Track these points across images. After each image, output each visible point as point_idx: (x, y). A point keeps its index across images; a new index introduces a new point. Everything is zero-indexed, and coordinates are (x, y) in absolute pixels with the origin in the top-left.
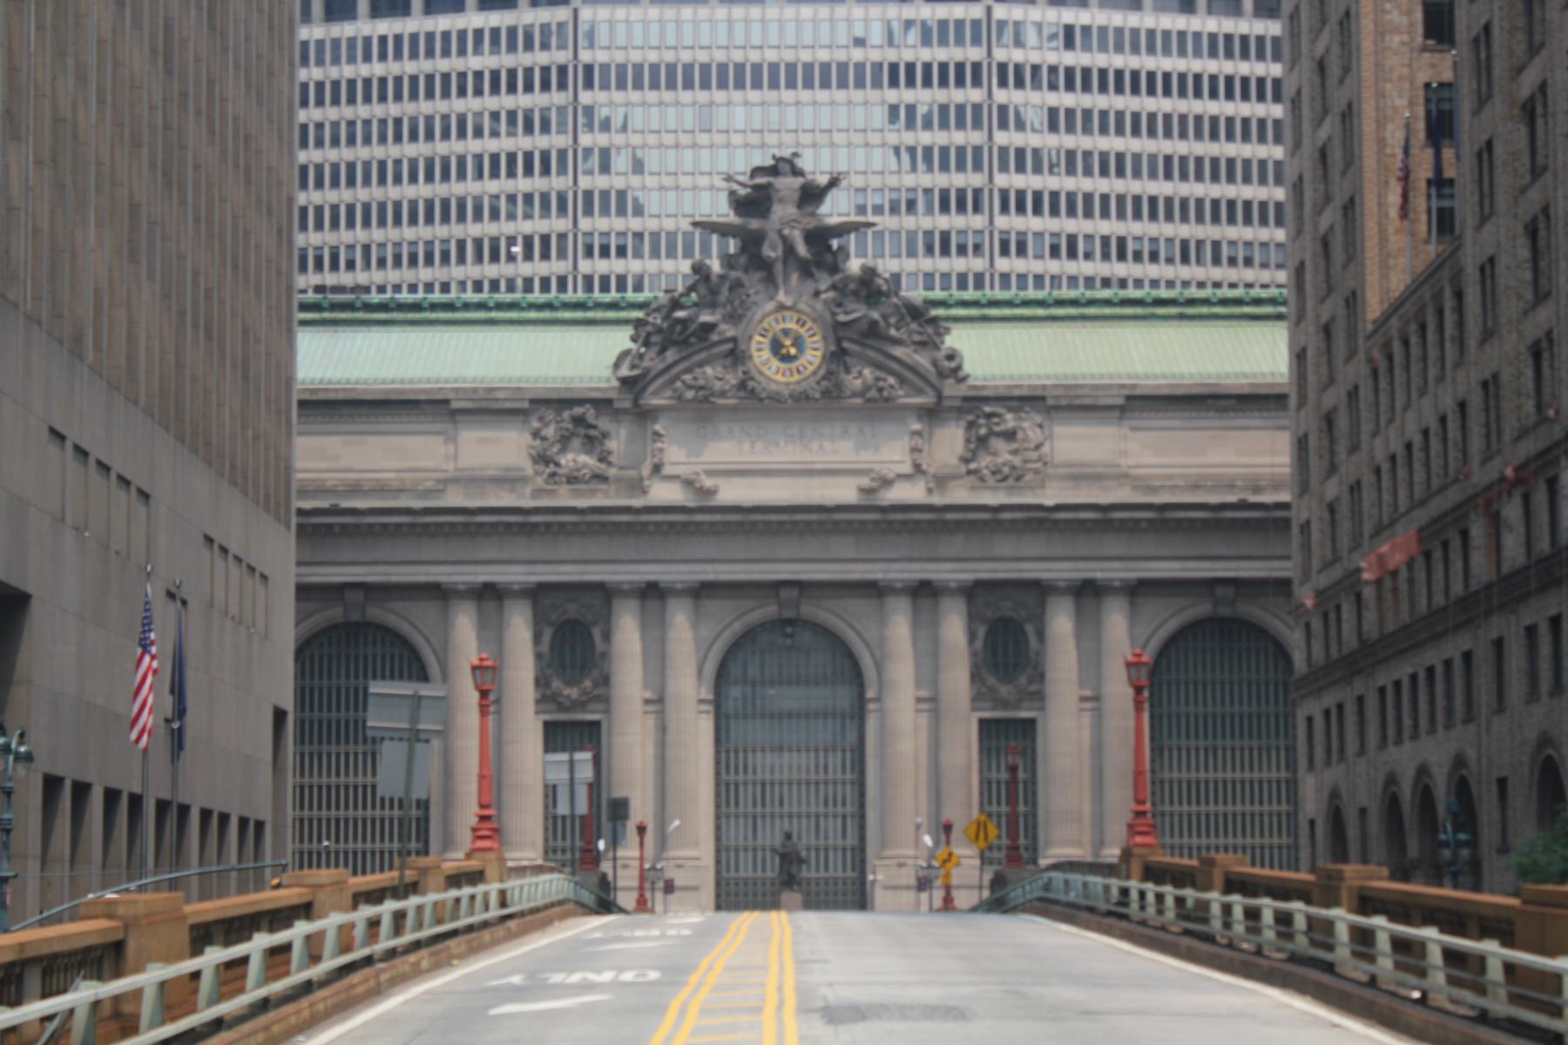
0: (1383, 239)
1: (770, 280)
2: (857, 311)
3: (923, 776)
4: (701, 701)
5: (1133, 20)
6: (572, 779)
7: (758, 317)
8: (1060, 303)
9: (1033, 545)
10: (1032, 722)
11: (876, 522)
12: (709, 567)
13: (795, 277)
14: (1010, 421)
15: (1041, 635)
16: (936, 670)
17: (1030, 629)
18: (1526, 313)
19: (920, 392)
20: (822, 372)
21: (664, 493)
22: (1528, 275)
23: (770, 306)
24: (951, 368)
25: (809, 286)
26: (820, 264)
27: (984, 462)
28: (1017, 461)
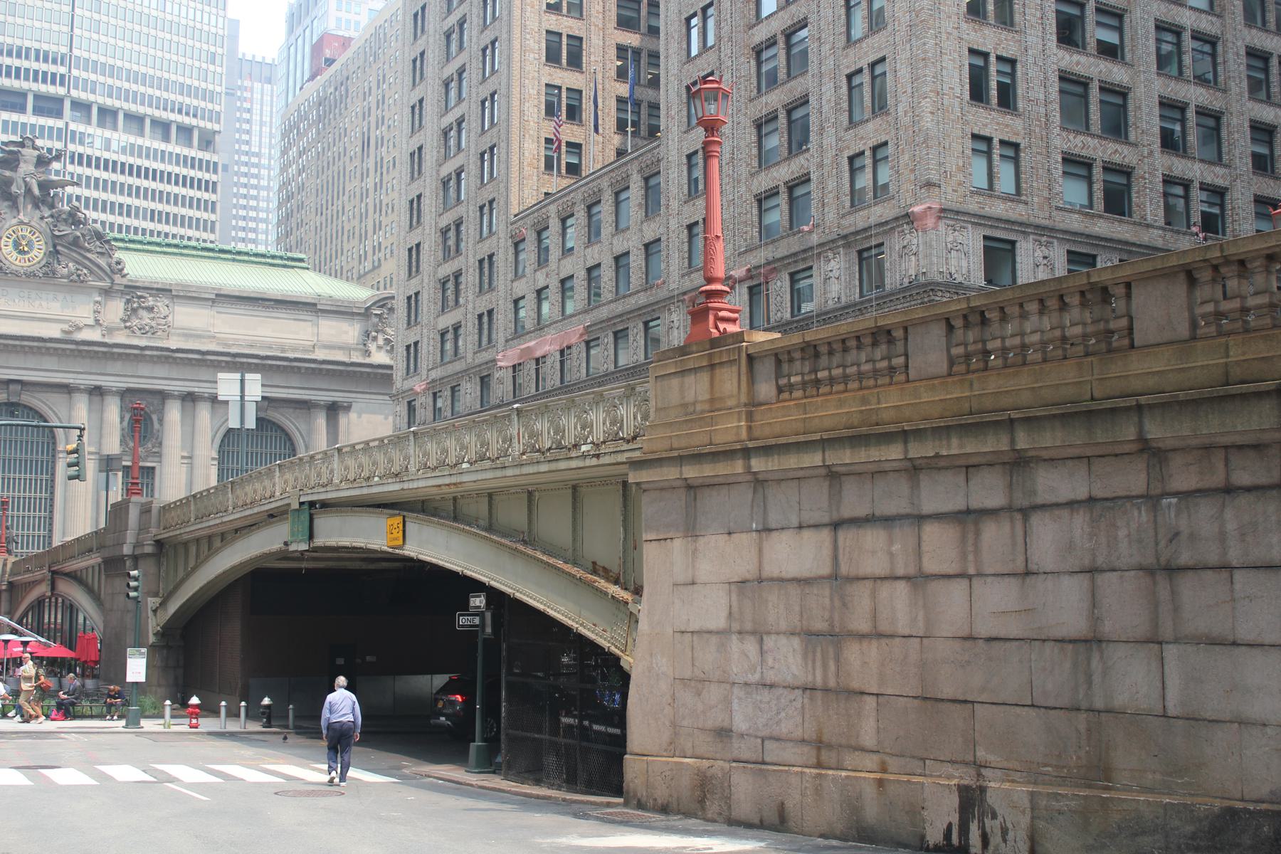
0: (521, 169)
1: (14, 206)
2: (66, 230)
3: (90, 496)
5: (140, 141)
6: (242, 397)
7: (7, 226)
8: (168, 245)
9: (161, 371)
10: (153, 468)
11: (72, 350)
13: (30, 207)
14: (151, 302)
15: (161, 421)
16: (101, 437)
17: (155, 417)
18: (752, 175)
19: (101, 279)
20: (43, 262)
22: (755, 151)
23: (15, 221)
24: (118, 269)
25: (37, 214)
26: (43, 202)
27: (135, 322)
28: (153, 324)
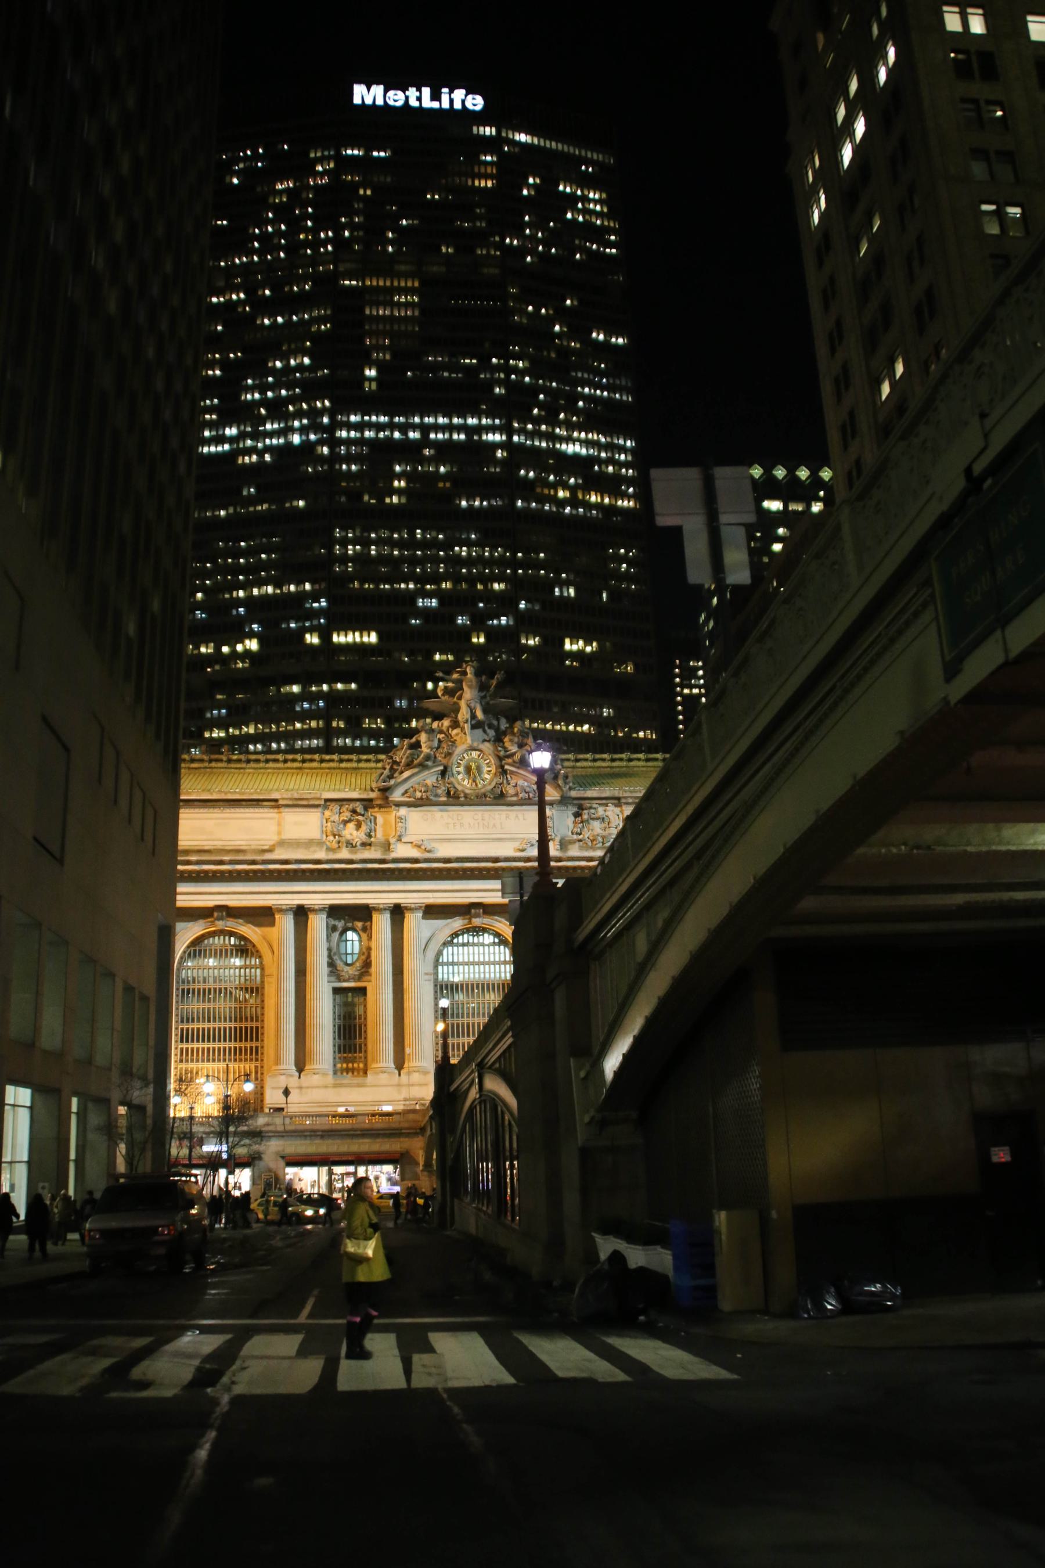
4: (426, 974)
12: (430, 895)
14: (601, 811)
21: (402, 851)
